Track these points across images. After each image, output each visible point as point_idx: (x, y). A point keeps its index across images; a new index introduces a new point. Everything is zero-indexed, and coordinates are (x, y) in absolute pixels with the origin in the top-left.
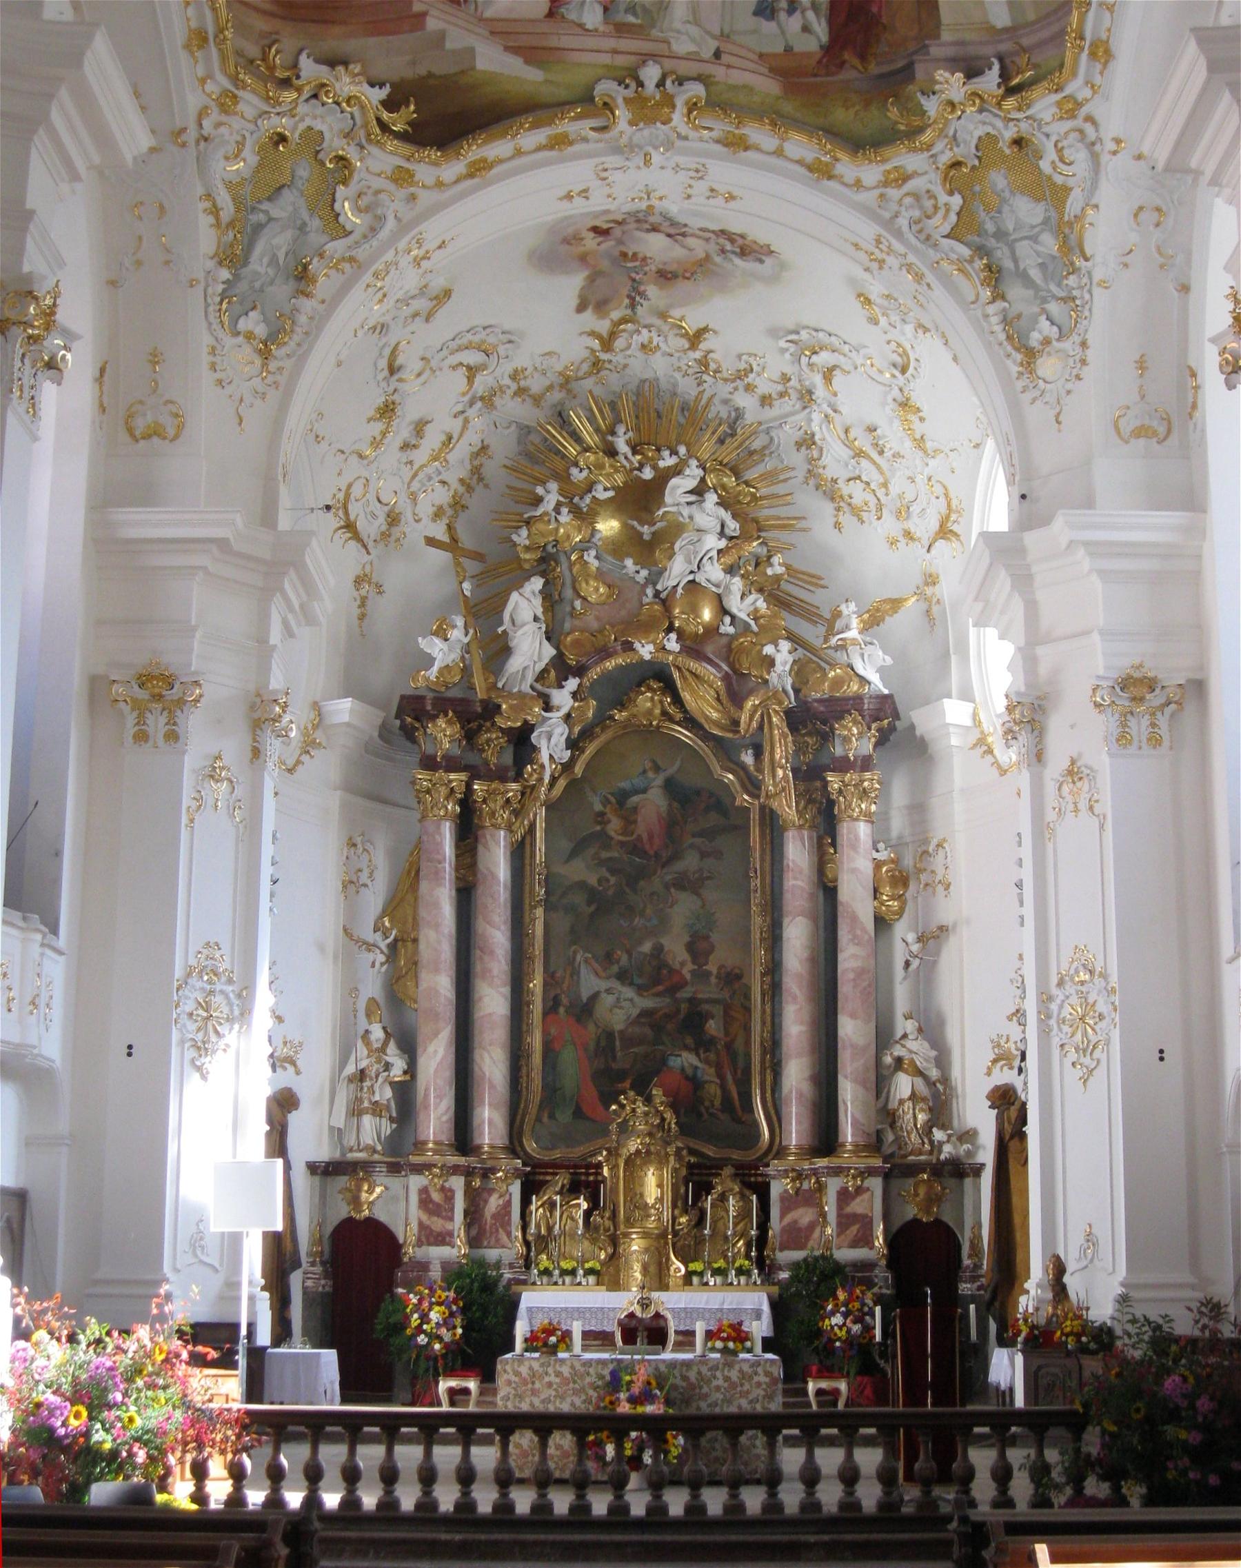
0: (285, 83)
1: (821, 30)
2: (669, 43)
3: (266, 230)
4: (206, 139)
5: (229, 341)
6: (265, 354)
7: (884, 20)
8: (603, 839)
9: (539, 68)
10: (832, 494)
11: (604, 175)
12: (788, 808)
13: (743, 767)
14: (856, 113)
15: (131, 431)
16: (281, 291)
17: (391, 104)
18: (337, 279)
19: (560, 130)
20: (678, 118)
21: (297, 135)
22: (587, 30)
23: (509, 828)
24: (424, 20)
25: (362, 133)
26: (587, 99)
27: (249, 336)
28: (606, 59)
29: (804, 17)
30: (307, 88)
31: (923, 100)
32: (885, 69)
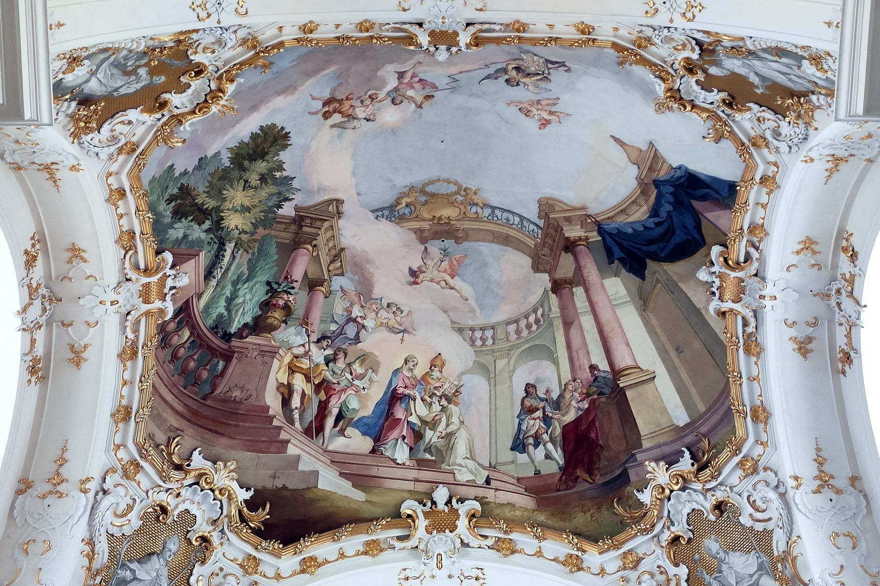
7: (601, 442)
14: (592, 517)
19: (374, 537)
20: (462, 523)
26: (396, 516)
31: (640, 496)
32: (608, 478)
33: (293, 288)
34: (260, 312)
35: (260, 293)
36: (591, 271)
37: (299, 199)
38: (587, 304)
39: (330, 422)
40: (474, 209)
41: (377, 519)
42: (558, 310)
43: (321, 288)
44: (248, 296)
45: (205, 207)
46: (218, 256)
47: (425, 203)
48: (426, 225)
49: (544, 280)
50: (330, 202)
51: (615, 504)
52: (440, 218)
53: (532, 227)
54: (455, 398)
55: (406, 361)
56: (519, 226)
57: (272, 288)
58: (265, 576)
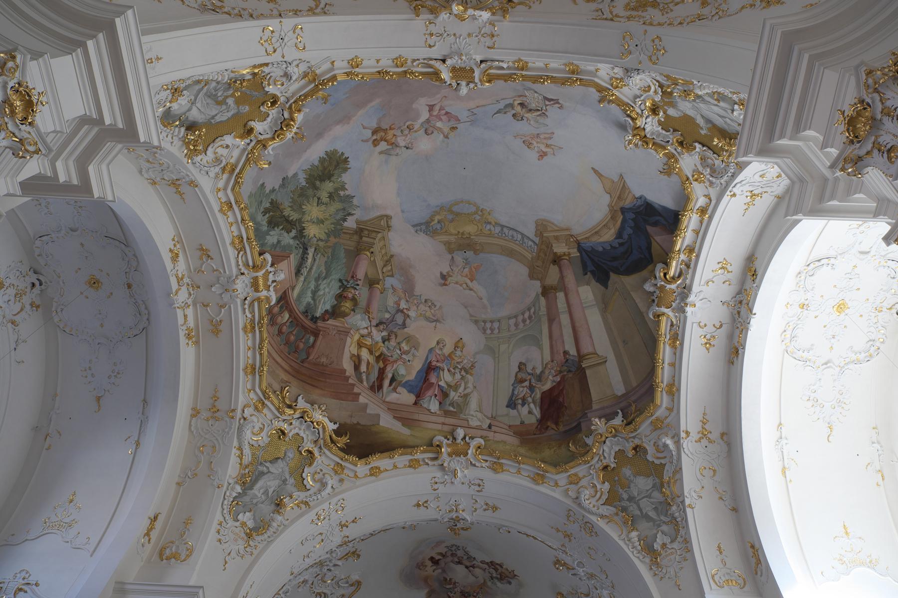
0: (290, 407)
1: (537, 412)
2: (468, 421)
3: (266, 476)
4: (245, 419)
5: (231, 523)
6: (249, 536)
9: (409, 429)
11: (436, 486)
14: (554, 452)
15: (161, 555)
16: (266, 509)
17: (338, 432)
18: (297, 511)
21: (290, 435)
22: (432, 413)
24: (358, 398)
25: (321, 442)
27: (244, 524)
28: (439, 427)
29: (529, 407)
30: (298, 411)
32: (567, 428)
33: (358, 285)
34: (336, 303)
35: (335, 289)
36: (570, 279)
37: (358, 214)
38: (566, 305)
39: (386, 383)
40: (488, 227)
41: (417, 447)
42: (545, 309)
43: (377, 286)
44: (327, 290)
45: (291, 218)
46: (303, 259)
47: (452, 221)
48: (452, 239)
49: (537, 286)
50: (381, 217)
51: (570, 445)
52: (463, 234)
53: (530, 243)
54: (470, 371)
55: (438, 343)
56: (521, 242)
57: (343, 284)
58: (348, 476)
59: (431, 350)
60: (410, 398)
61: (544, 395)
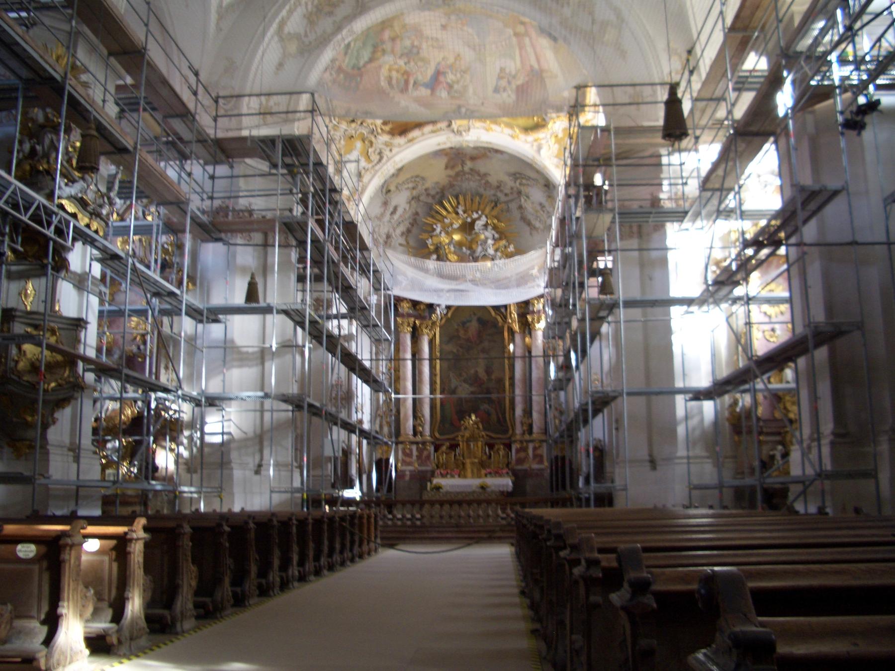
1: (513, 96)
8: (459, 337)
10: (529, 224)
12: (516, 327)
13: (502, 313)
23: (428, 334)
59: (439, 64)
60: (429, 92)
61: (518, 87)
